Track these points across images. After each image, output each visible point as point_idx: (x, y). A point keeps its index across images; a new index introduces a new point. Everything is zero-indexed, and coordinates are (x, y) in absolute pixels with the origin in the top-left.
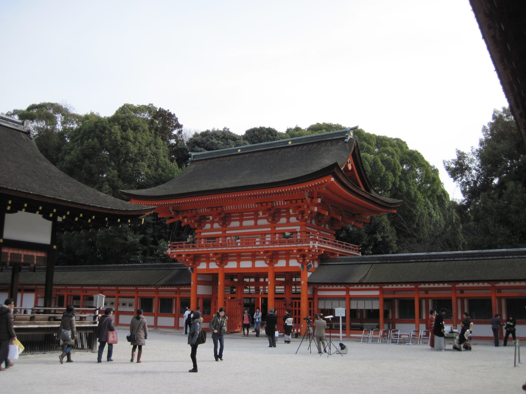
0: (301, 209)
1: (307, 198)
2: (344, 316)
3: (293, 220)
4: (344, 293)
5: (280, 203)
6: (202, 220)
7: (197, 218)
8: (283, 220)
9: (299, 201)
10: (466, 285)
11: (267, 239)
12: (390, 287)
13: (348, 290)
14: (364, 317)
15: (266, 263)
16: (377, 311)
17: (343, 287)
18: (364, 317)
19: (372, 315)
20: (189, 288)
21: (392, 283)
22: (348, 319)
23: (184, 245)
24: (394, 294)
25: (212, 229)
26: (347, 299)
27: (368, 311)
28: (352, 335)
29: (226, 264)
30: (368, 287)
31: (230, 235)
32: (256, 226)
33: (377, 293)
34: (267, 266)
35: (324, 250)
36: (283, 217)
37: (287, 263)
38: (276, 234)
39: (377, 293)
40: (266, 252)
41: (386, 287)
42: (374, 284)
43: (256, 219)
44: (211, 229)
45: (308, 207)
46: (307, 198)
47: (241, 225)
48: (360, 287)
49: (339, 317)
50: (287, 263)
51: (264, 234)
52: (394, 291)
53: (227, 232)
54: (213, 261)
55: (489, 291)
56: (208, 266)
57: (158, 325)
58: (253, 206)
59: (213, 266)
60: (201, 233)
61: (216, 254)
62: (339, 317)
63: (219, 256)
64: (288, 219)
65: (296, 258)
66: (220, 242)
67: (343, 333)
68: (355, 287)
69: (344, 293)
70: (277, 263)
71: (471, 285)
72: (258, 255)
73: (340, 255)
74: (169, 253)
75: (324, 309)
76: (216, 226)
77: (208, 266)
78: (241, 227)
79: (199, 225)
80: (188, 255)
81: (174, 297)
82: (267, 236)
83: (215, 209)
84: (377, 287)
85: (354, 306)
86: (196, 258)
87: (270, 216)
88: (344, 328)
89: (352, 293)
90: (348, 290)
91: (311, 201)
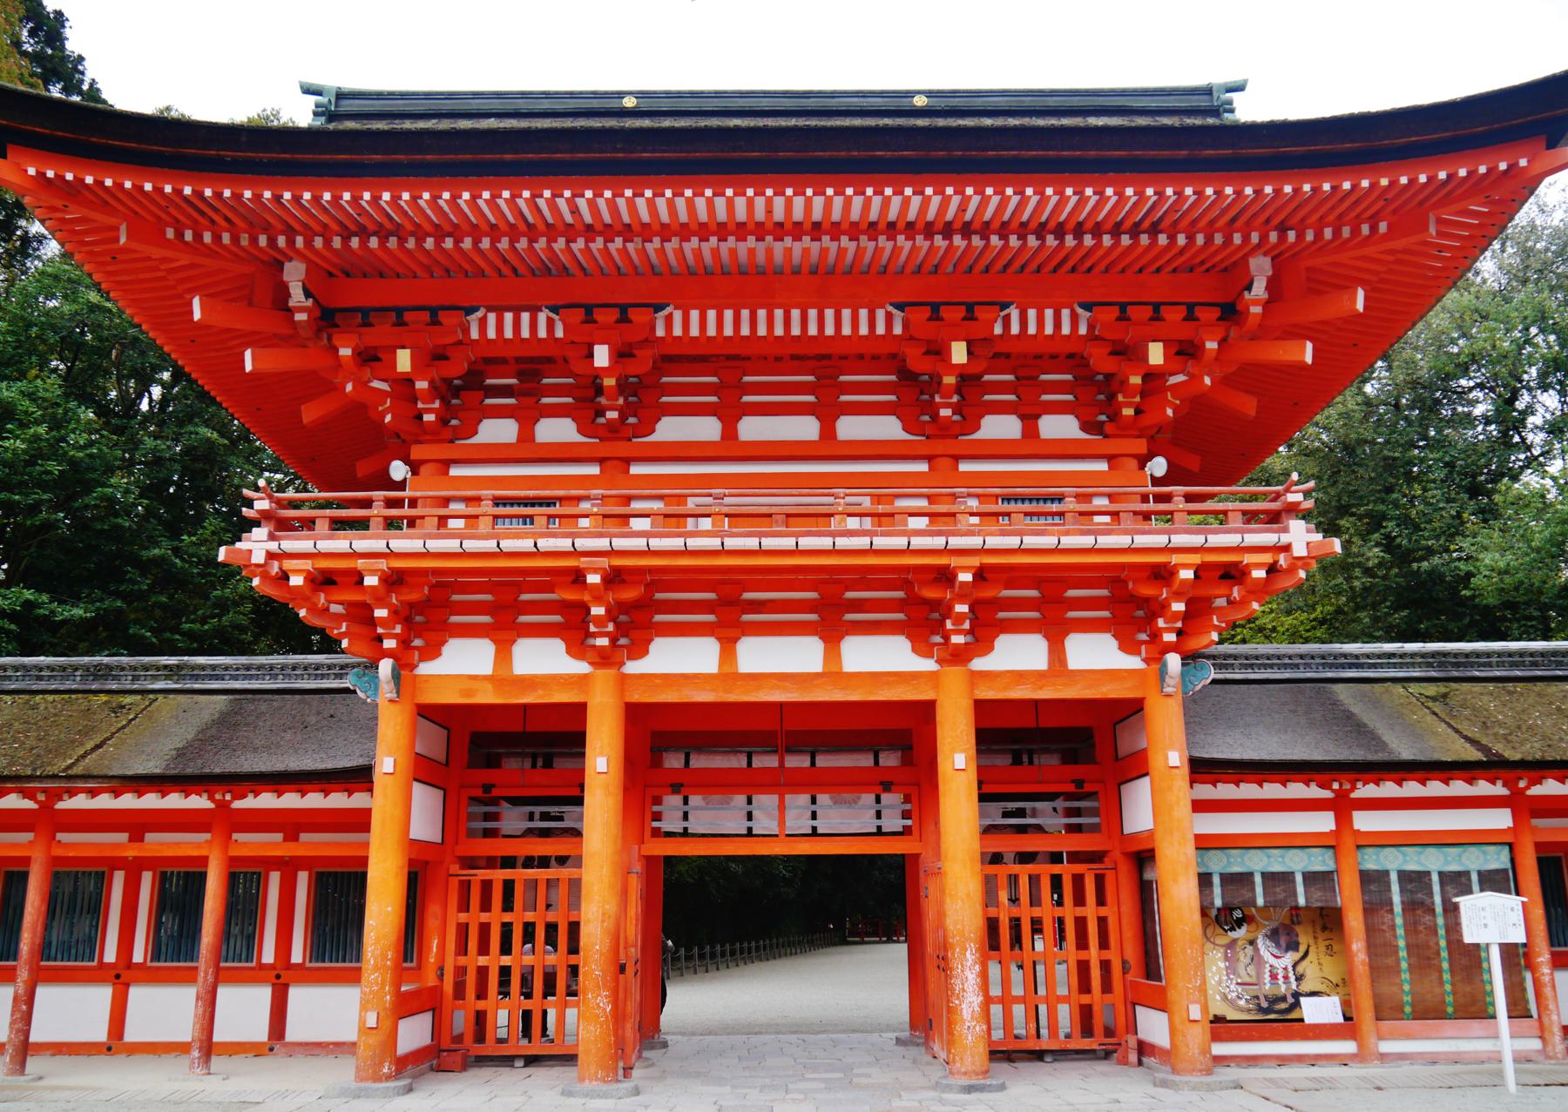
2: (1519, 937)
6: (468, 386)
13: (1342, 807)
20: (358, 800)
23: (378, 510)
28: (1386, 1047)
32: (828, 447)
39: (1501, 819)
57: (35, 1036)
59: (543, 660)
60: (447, 464)
64: (1030, 422)
69: (1323, 822)
74: (258, 558)
78: (730, 448)
80: (394, 580)
81: (116, 863)
86: (431, 604)
89: (1364, 821)
90: (1342, 807)
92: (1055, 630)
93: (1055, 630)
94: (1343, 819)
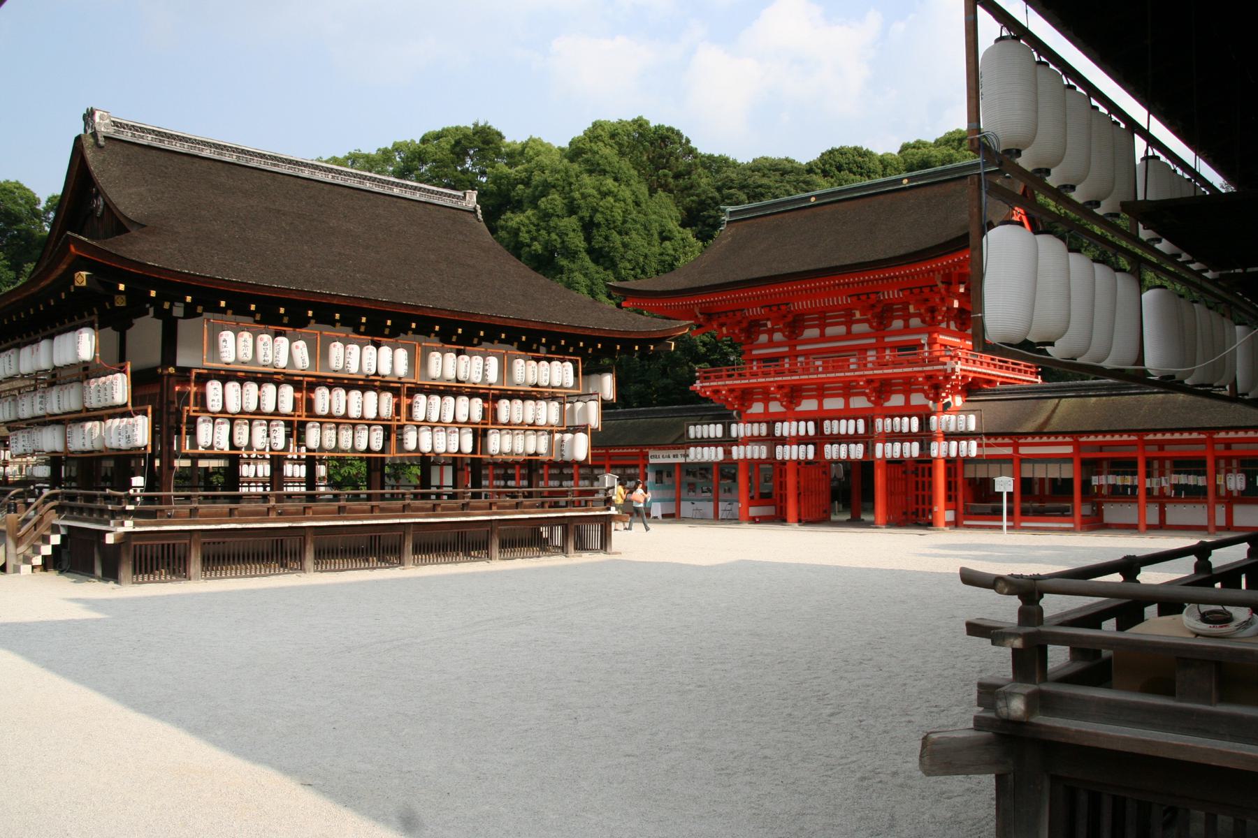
0: (930, 304)
1: (940, 285)
3: (915, 322)
4: (1008, 451)
5: (893, 294)
6: (753, 328)
7: (744, 325)
8: (898, 324)
9: (927, 290)
10: (1168, 436)
11: (869, 359)
12: (1092, 438)
13: (1016, 446)
14: (1047, 492)
15: (869, 400)
16: (1068, 482)
17: (1007, 440)
18: (1047, 492)
19: (1061, 488)
21: (1096, 433)
22: (1017, 497)
24: (1101, 451)
25: (771, 343)
26: (1016, 461)
27: (1054, 480)
28: (1023, 524)
29: (799, 404)
30: (1052, 439)
31: (806, 354)
32: (849, 335)
33: (1068, 450)
34: (870, 405)
35: (972, 375)
36: (898, 317)
37: (907, 400)
38: (884, 349)
40: (869, 381)
41: (1084, 439)
42: (1064, 434)
43: (849, 323)
44: (770, 342)
45: (942, 300)
46: (940, 285)
47: (822, 334)
48: (1037, 440)
49: (1001, 493)
50: (907, 400)
51: (863, 350)
52: (1101, 446)
53: (799, 348)
54: (775, 399)
55: (1202, 447)
56: (766, 407)
58: (843, 300)
61: (780, 387)
62: (1001, 493)
63: (785, 391)
65: (922, 391)
66: (787, 366)
67: (1008, 520)
68: (1029, 440)
70: (888, 399)
71: (1177, 436)
72: (855, 387)
73: (1002, 383)
75: (975, 479)
76: (778, 336)
77: (766, 407)
78: (823, 338)
79: (748, 337)
80: (731, 391)
82: (869, 353)
83: (775, 309)
84: (1068, 439)
85: (1027, 471)
87: (873, 317)
88: (1010, 512)
90: (1016, 446)
91: (948, 290)
92: (907, 393)
93: (907, 393)
94: (1016, 451)
